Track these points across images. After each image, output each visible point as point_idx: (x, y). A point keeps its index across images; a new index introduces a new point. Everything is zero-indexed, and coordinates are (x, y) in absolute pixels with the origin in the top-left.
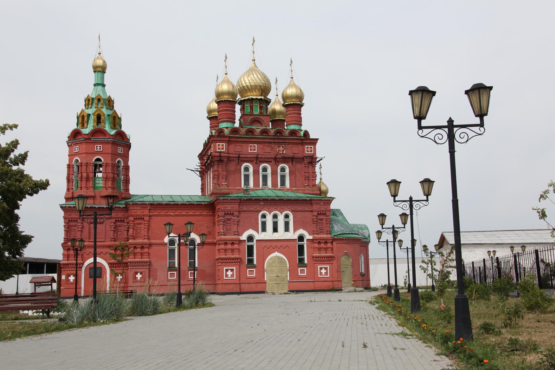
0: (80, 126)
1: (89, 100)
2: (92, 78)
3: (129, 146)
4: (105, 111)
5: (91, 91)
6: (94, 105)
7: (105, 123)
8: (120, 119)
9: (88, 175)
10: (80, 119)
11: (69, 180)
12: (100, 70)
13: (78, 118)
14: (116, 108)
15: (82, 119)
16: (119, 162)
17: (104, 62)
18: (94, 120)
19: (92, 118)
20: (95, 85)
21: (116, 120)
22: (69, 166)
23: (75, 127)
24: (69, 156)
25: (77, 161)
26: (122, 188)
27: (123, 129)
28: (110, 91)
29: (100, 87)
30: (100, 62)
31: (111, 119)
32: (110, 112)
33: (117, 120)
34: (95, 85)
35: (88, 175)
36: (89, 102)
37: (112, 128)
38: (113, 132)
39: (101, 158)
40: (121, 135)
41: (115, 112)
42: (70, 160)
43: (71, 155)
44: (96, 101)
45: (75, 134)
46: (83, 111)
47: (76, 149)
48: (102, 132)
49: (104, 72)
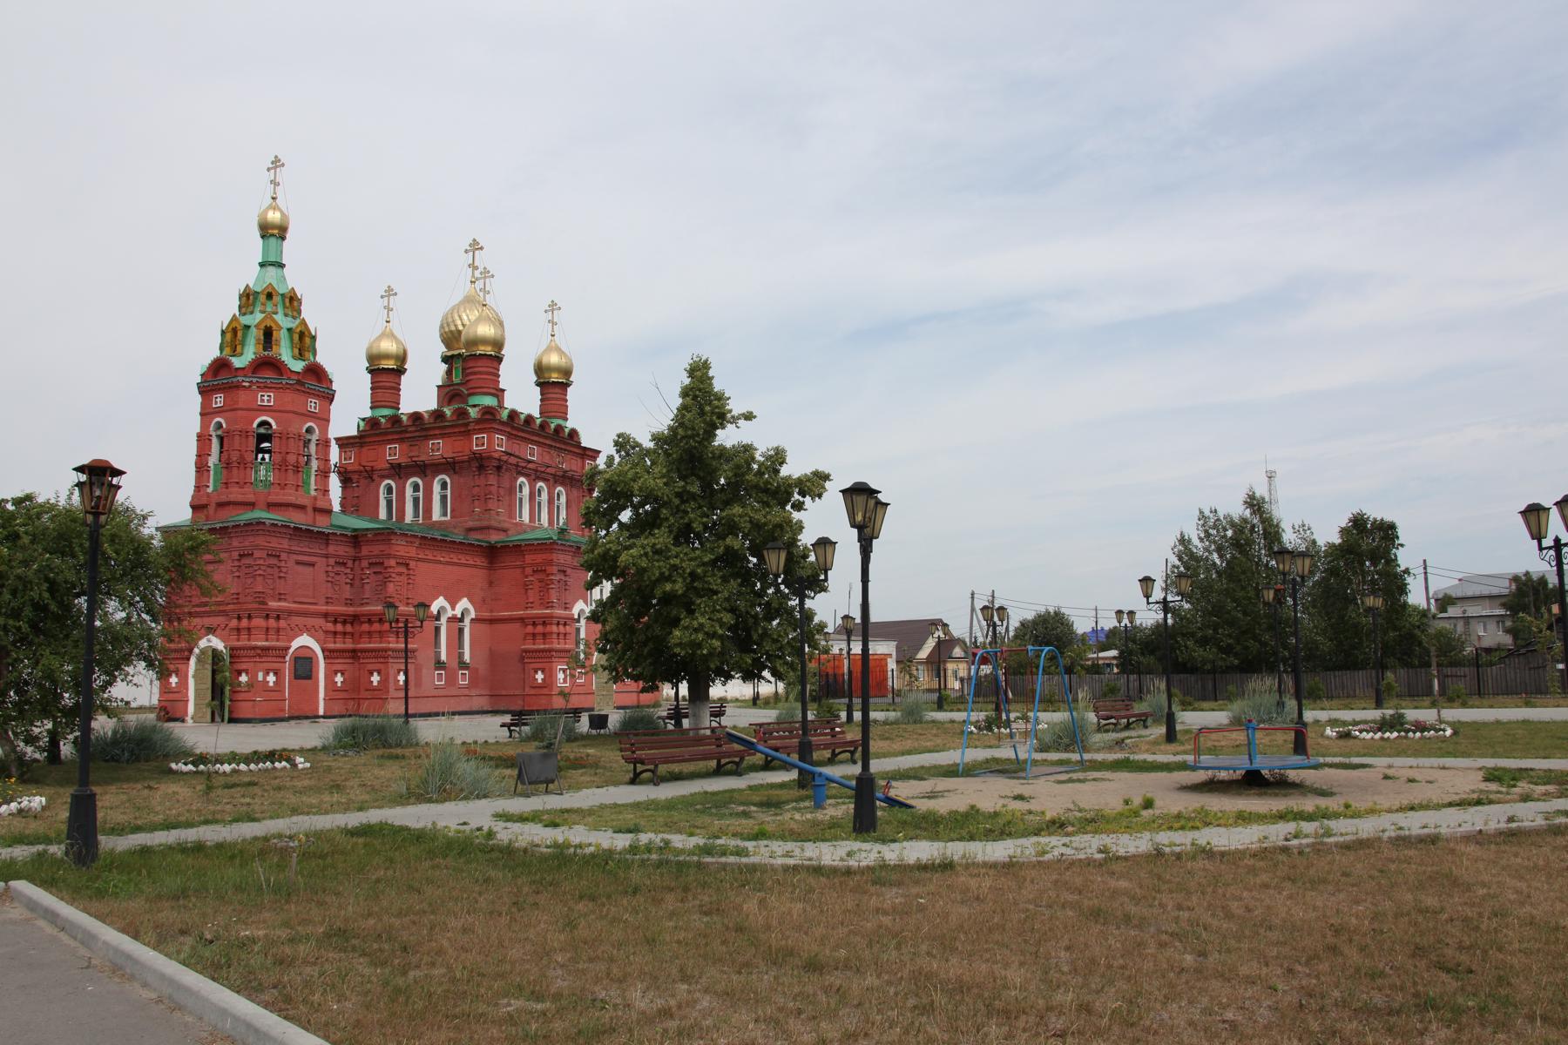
0: (227, 351)
1: (248, 296)
2: (255, 247)
3: (329, 397)
4: (283, 321)
5: (250, 275)
6: (258, 309)
7: (278, 345)
8: (314, 338)
9: (242, 457)
10: (229, 336)
11: (201, 468)
12: (273, 232)
13: (223, 333)
14: (306, 313)
15: (233, 336)
16: (309, 430)
17: (282, 213)
18: (258, 340)
19: (254, 336)
20: (262, 265)
21: (304, 340)
22: (203, 439)
23: (217, 354)
24: (202, 414)
25: (219, 426)
26: (313, 486)
27: (321, 359)
28: (294, 278)
29: (271, 270)
30: (274, 217)
31: (296, 337)
32: (293, 324)
33: (307, 340)
34: (262, 265)
35: (242, 457)
36: (248, 299)
37: (294, 357)
38: (298, 366)
39: (270, 420)
40: (317, 373)
41: (304, 323)
42: (204, 425)
43: (206, 413)
44: (262, 298)
45: (219, 367)
46: (234, 318)
47: (219, 400)
48: (275, 365)
49: (283, 238)
